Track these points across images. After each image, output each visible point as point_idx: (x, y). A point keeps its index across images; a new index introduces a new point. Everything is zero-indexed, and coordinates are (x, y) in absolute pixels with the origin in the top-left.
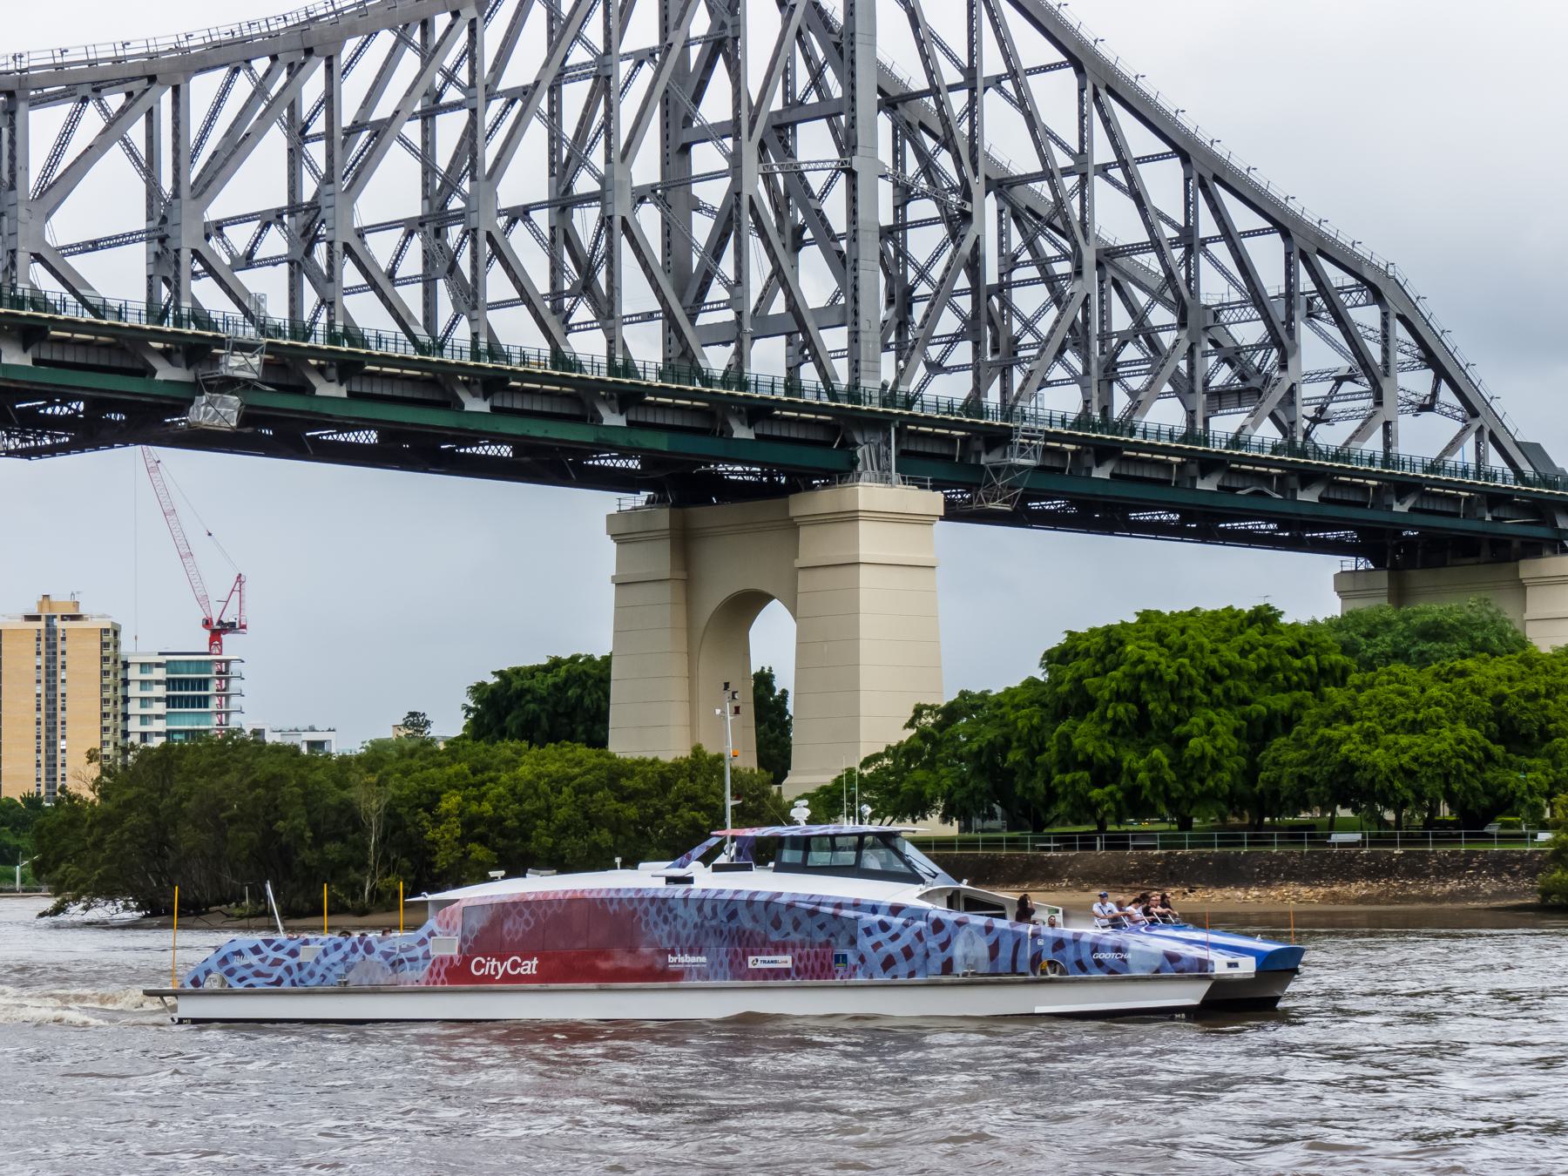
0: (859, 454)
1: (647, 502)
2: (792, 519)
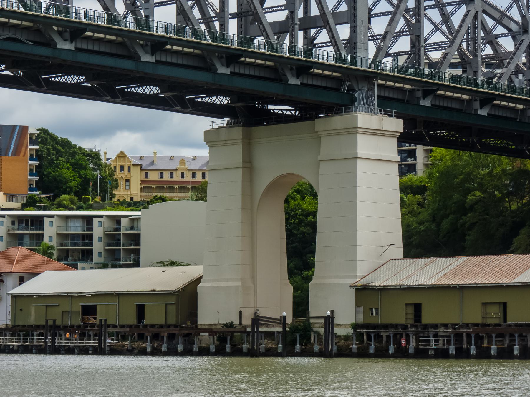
0: (356, 95)
1: (227, 124)
2: (317, 132)
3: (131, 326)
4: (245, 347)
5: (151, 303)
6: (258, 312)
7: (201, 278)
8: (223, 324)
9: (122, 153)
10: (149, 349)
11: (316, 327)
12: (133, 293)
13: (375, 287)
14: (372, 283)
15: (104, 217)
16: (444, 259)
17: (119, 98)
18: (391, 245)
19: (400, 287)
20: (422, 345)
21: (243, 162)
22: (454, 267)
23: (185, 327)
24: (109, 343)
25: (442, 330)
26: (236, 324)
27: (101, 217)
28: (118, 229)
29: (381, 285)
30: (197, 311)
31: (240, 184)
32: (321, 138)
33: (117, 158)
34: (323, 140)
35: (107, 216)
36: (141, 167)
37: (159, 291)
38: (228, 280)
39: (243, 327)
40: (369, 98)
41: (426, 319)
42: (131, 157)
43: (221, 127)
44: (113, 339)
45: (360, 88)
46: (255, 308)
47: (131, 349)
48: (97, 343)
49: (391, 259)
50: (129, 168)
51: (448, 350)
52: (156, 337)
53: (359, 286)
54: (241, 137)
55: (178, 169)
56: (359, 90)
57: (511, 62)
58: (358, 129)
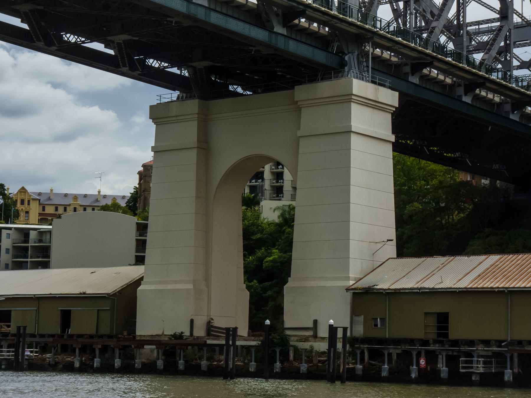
0: (346, 58)
1: (178, 98)
2: (297, 102)
3: (53, 336)
4: (204, 363)
5: (80, 309)
6: (212, 321)
7: (142, 279)
8: (171, 335)
9: (23, 188)
10: (77, 365)
11: (292, 341)
12: (57, 296)
13: (381, 291)
14: (377, 285)
15: (13, 229)
16: (466, 258)
17: (54, 45)
18: (388, 240)
19: (419, 291)
20: (463, 368)
21: (199, 140)
22: (488, 266)
23: (121, 338)
24: (27, 355)
25: (480, 347)
26: (186, 336)
27: (10, 229)
28: (26, 240)
29: (392, 287)
30: (136, 318)
31: (194, 168)
32: (301, 110)
33: (19, 193)
34: (305, 112)
35: (15, 228)
36: (39, 202)
37: (90, 294)
38: (176, 282)
39: (194, 339)
40: (361, 62)
41: (453, 334)
42: (31, 193)
43: (172, 102)
44: (33, 351)
45: (350, 50)
46: (208, 316)
47: (54, 363)
48: (12, 355)
49: (390, 258)
50: (29, 201)
51: (502, 374)
52: (84, 349)
53: (360, 289)
54: (197, 111)
55: (71, 204)
56: (349, 53)
57: (493, 48)
58: (353, 97)
